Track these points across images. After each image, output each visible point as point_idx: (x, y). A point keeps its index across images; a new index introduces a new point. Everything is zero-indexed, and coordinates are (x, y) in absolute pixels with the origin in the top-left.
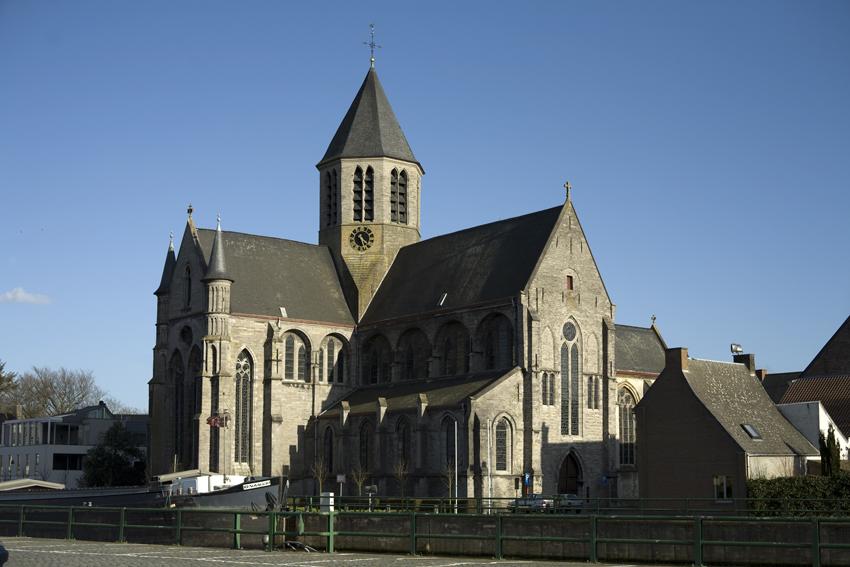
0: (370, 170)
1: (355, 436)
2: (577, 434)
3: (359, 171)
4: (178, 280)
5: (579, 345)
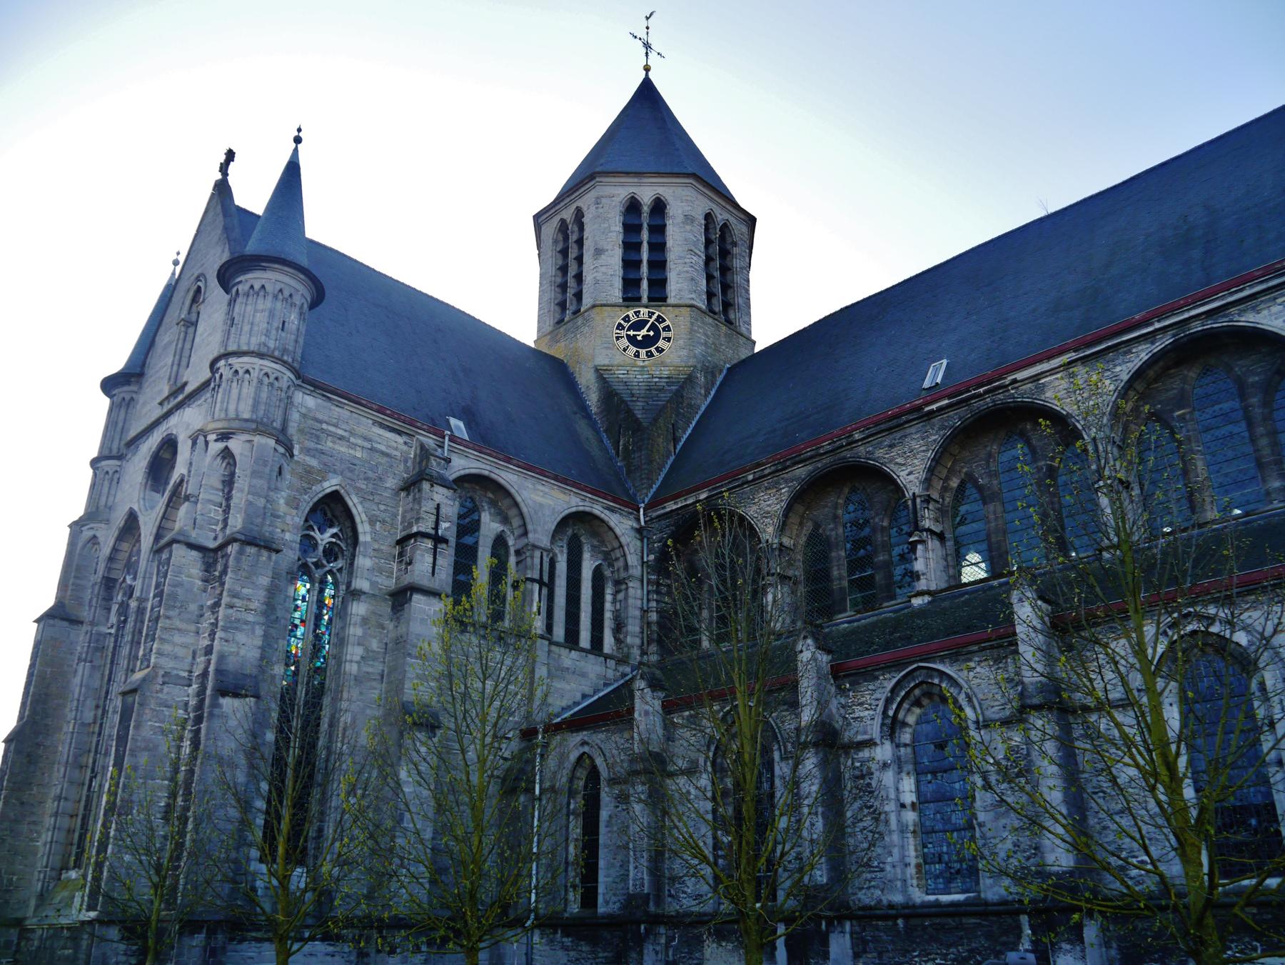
0: (659, 207)
1: (691, 772)
3: (633, 206)
4: (169, 336)
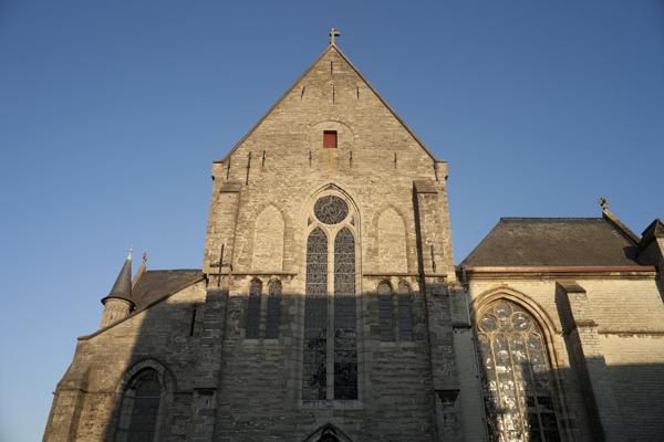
2: (353, 396)
5: (354, 229)
